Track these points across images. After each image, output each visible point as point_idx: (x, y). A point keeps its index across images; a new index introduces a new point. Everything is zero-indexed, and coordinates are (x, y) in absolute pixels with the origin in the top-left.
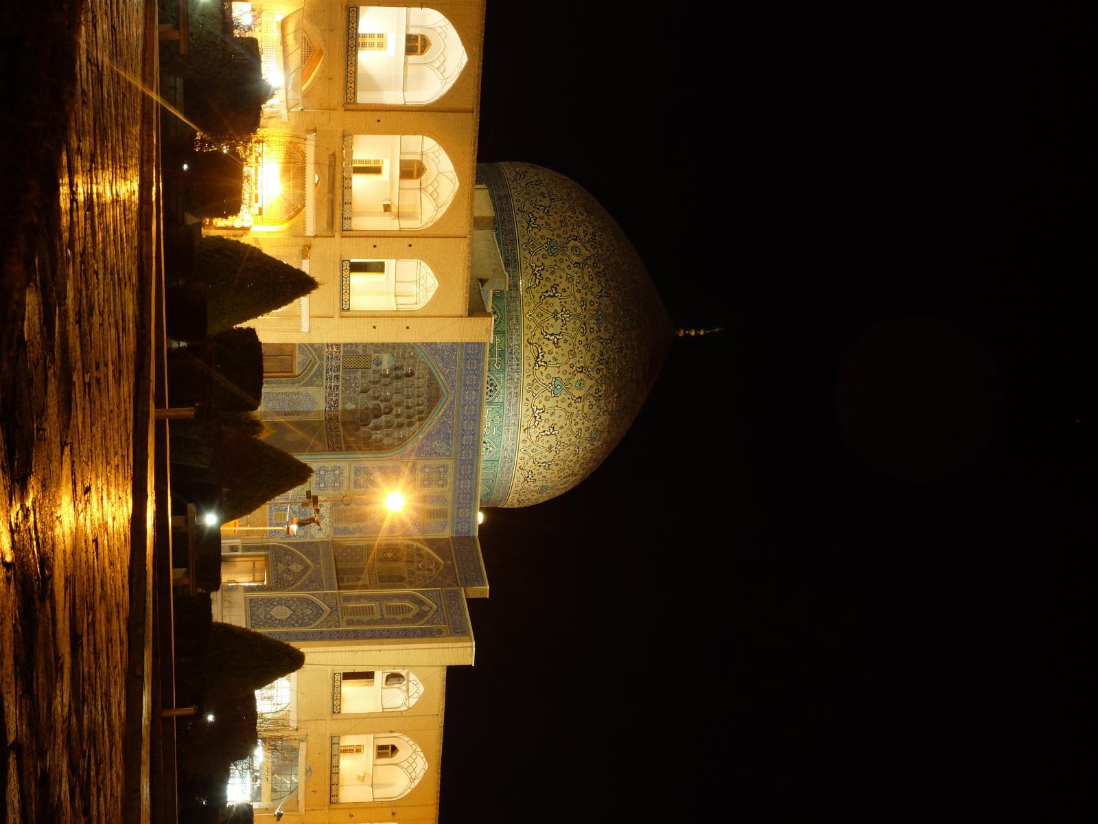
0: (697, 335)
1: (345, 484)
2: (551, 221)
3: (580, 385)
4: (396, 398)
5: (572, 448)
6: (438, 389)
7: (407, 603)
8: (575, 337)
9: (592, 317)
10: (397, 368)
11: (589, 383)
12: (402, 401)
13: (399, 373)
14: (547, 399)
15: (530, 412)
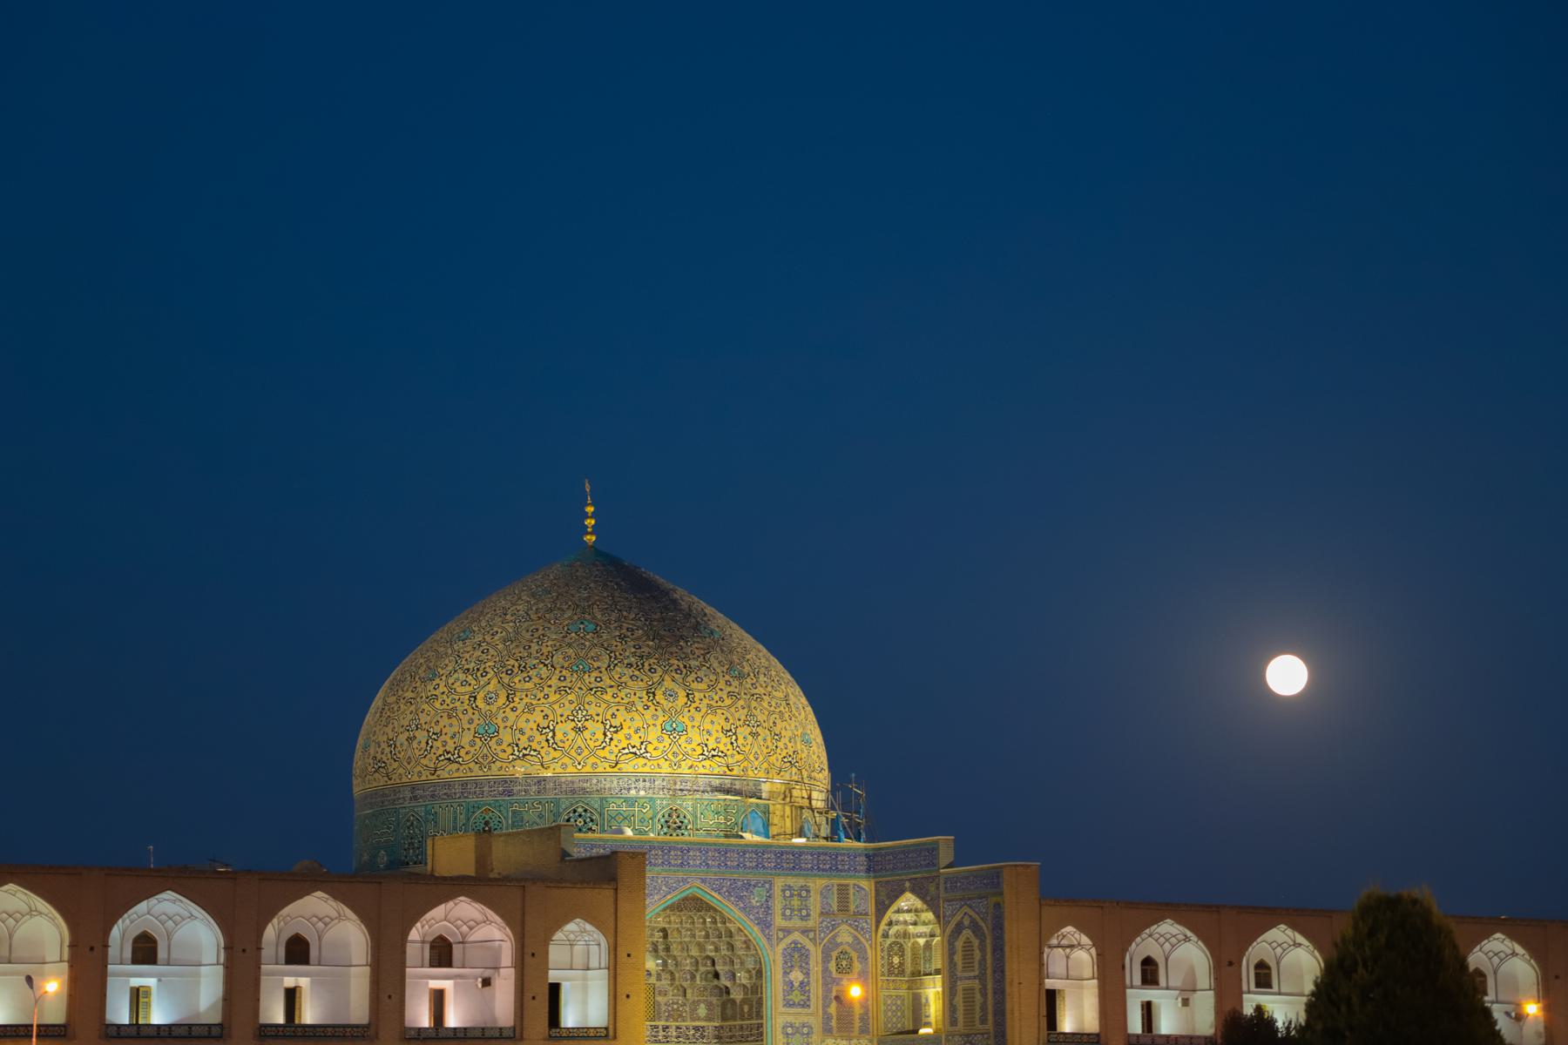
0: (593, 516)
1: (805, 1019)
2: (450, 731)
3: (671, 695)
4: (695, 952)
5: (754, 704)
6: (685, 899)
7: (959, 944)
8: (605, 701)
9: (581, 679)
10: (656, 950)
11: (668, 683)
12: (699, 944)
13: (661, 947)
14: (689, 741)
15: (707, 763)
